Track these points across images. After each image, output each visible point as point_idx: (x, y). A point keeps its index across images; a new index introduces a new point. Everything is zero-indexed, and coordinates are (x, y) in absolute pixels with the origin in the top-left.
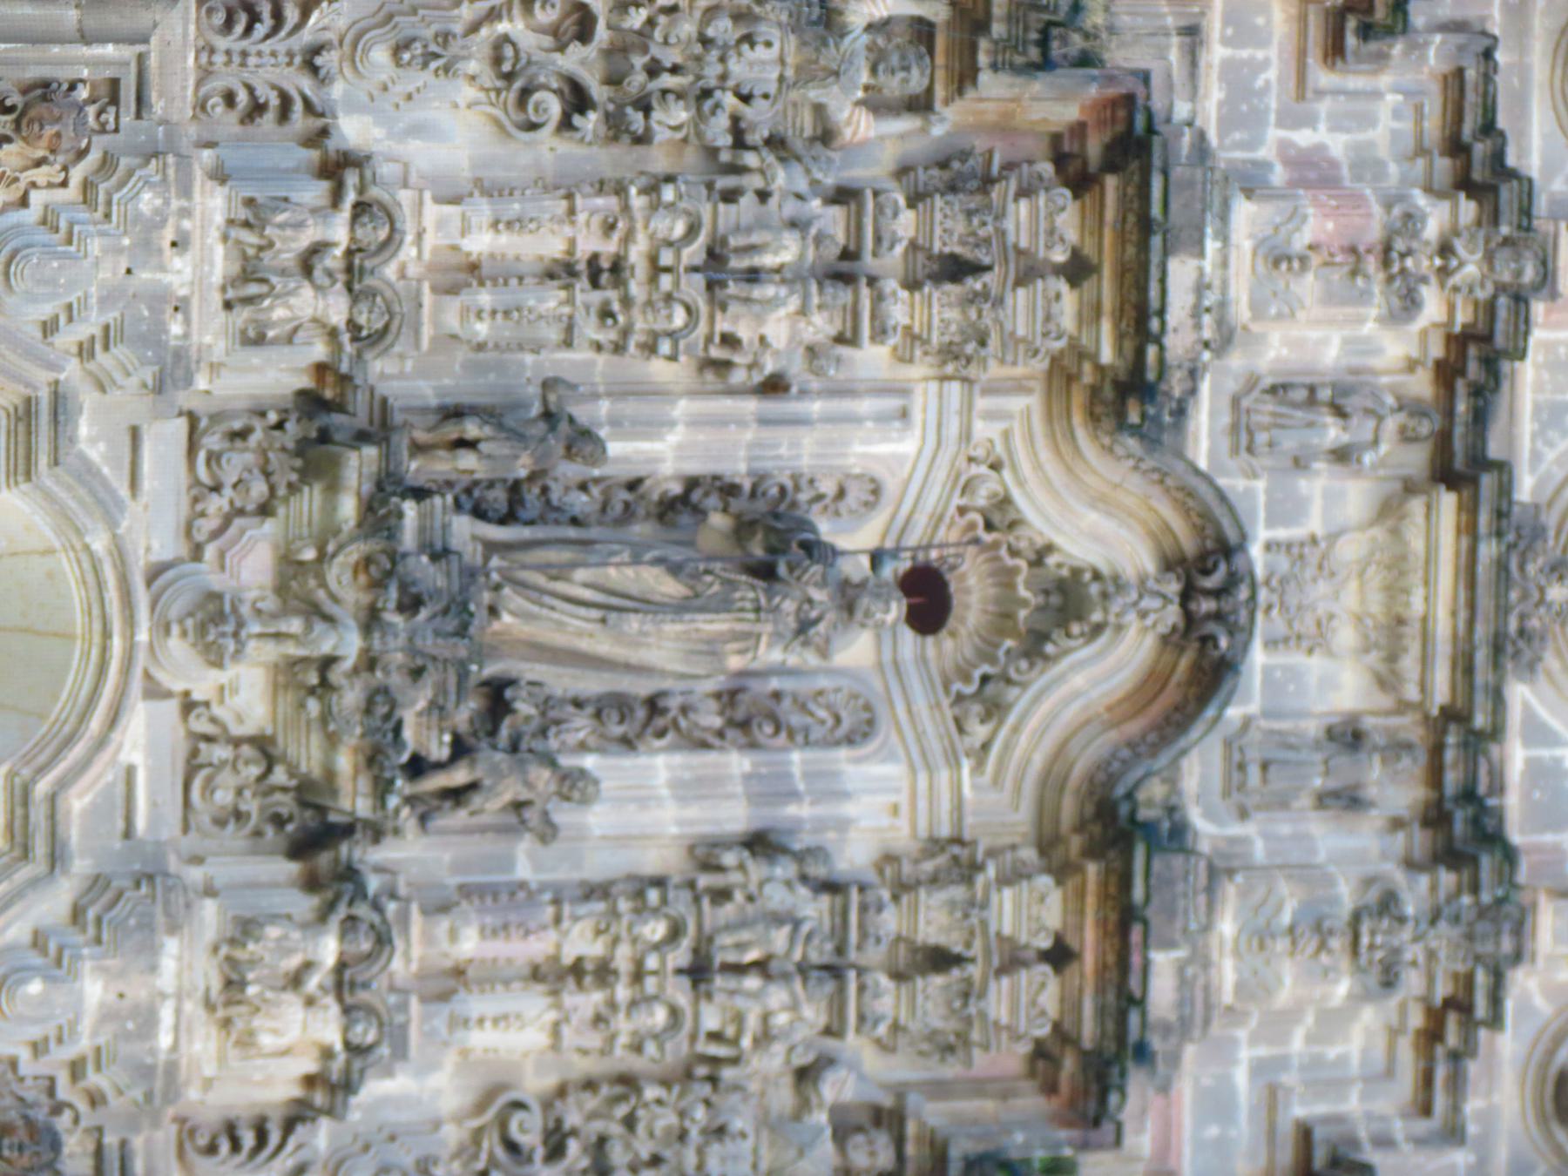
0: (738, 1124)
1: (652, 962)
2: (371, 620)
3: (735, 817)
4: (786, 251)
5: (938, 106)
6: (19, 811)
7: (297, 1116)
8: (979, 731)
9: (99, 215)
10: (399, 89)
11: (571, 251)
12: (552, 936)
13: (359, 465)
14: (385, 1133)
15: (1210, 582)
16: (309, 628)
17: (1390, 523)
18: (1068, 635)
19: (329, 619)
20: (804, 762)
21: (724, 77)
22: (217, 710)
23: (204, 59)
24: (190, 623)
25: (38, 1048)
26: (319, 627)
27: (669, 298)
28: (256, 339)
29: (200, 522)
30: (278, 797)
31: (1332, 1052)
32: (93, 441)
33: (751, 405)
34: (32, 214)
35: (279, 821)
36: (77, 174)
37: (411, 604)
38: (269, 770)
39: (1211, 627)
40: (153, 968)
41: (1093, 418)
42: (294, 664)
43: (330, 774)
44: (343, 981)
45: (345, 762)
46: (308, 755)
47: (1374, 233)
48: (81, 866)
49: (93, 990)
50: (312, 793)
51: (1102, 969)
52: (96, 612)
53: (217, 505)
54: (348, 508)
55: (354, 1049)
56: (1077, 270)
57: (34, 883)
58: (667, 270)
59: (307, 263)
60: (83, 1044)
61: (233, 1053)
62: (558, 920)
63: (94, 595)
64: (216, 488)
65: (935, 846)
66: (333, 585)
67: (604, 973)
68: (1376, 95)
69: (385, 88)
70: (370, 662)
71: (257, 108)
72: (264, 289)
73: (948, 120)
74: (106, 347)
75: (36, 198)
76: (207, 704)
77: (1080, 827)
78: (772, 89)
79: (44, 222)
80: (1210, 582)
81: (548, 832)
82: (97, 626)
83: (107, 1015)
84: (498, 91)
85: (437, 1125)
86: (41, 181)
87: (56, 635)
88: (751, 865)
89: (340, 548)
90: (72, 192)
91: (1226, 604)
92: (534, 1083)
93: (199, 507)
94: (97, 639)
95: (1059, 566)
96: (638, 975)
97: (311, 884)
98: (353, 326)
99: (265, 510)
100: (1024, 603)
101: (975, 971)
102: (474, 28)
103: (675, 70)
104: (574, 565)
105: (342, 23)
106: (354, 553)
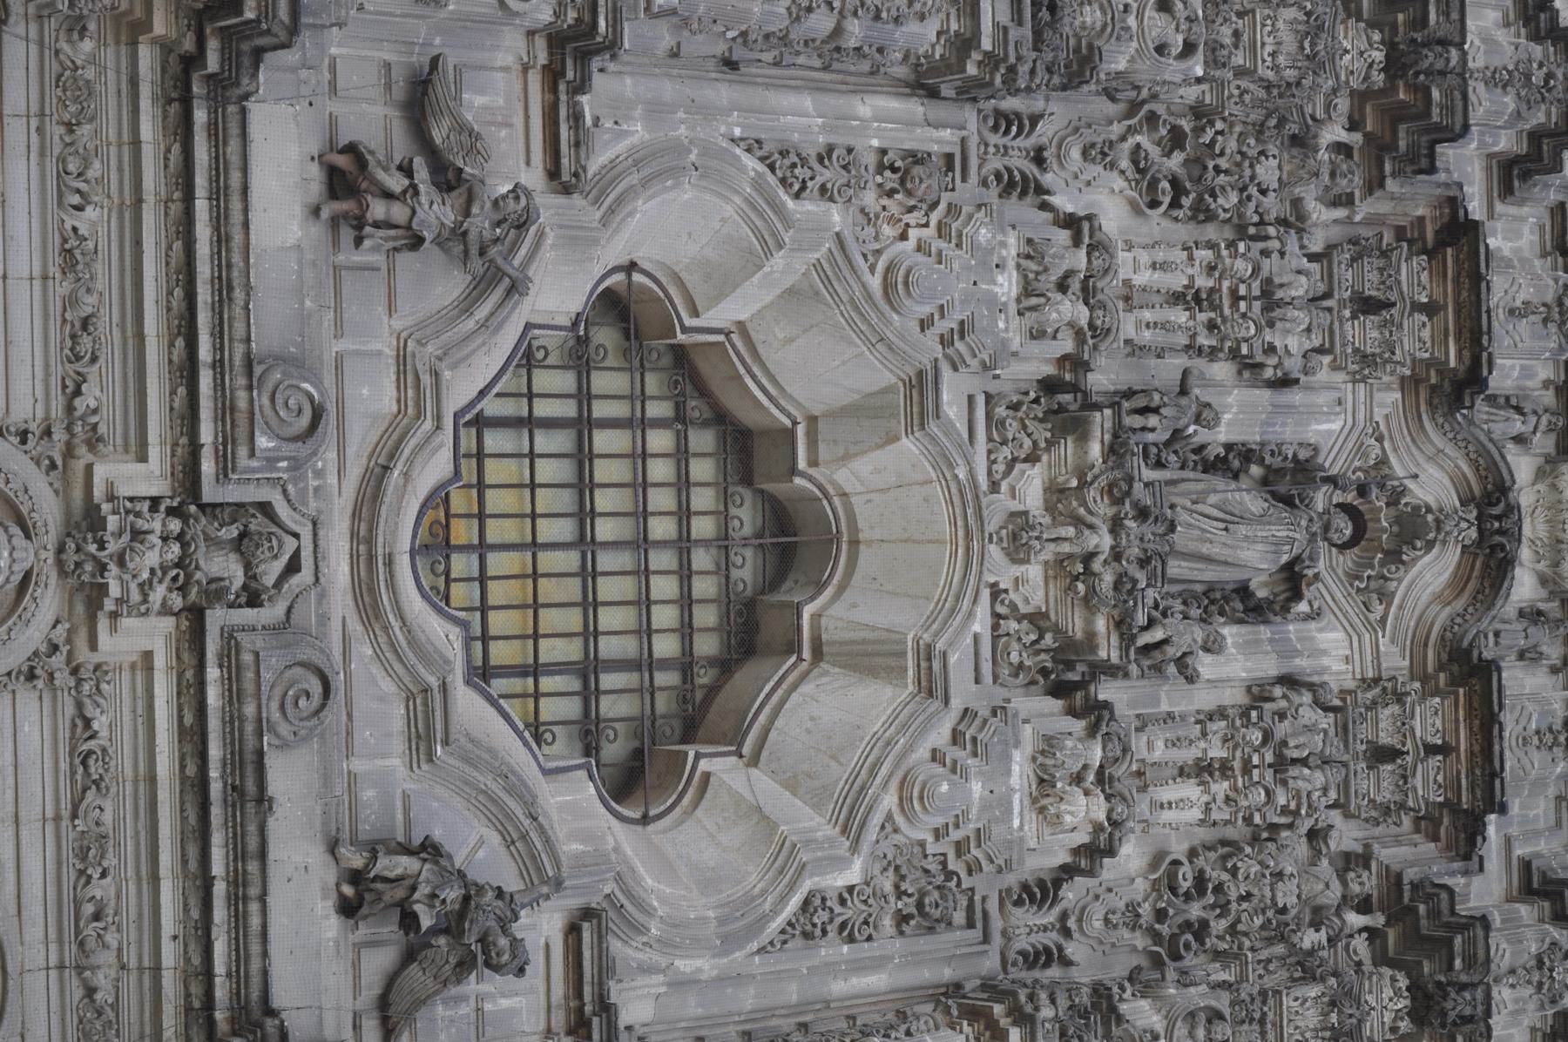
0: (1289, 869)
1: (1256, 760)
2: (1116, 526)
3: (1270, 667)
4: (1300, 288)
5: (1357, 202)
6: (924, 664)
7: (1067, 872)
8: (1379, 609)
9: (953, 245)
10: (1085, 177)
11: (1186, 287)
12: (1202, 744)
13: (1101, 422)
14: (1104, 886)
15: (1496, 511)
16: (1079, 534)
17: (1548, 481)
18: (1414, 548)
19: (1091, 527)
20: (1296, 631)
21: (1252, 178)
22: (1013, 596)
23: (982, 148)
24: (1004, 532)
25: (938, 834)
26: (1087, 532)
27: (1244, 316)
28: (1037, 334)
29: (995, 467)
30: (1043, 656)
31: (1532, 813)
32: (950, 404)
33: (1265, 395)
34: (910, 244)
35: (1044, 672)
36: (934, 217)
37: (1142, 514)
38: (1041, 637)
39: (1498, 539)
40: (1008, 773)
41: (1432, 407)
42: (1061, 562)
43: (1091, 635)
44: (1102, 778)
45: (1101, 624)
46: (1076, 625)
47: (1550, 297)
48: (957, 703)
49: (977, 788)
50: (1070, 651)
51: (1471, 754)
52: (960, 523)
53: (1006, 452)
54: (1095, 450)
55: (1115, 824)
56: (1431, 309)
57: (938, 712)
58: (1243, 298)
59: (1062, 287)
60: (968, 830)
61: (1047, 831)
62: (1204, 734)
63: (958, 511)
64: (1004, 443)
65: (1367, 683)
66: (1091, 505)
67: (1225, 768)
68: (1523, 219)
69: (1076, 177)
70: (1117, 555)
71: (1011, 184)
72: (1042, 300)
73: (1363, 210)
74: (962, 337)
75: (913, 234)
76: (1006, 591)
77: (1440, 667)
78: (1276, 185)
79: (919, 249)
80: (1496, 511)
81: (1191, 679)
82: (961, 533)
83: (985, 806)
84: (1137, 182)
85: (1133, 880)
86: (913, 222)
87: (930, 542)
88: (1290, 694)
89: (1096, 477)
90: (930, 232)
91: (1506, 524)
92: (1179, 849)
93: (993, 457)
94: (961, 542)
95: (1406, 504)
96: (1247, 768)
97: (1072, 712)
98: (1091, 325)
99: (1032, 459)
100: (1384, 530)
101: (1409, 759)
102: (1123, 139)
103: (1226, 172)
104: (1207, 492)
105: (1050, 133)
106: (1103, 482)
